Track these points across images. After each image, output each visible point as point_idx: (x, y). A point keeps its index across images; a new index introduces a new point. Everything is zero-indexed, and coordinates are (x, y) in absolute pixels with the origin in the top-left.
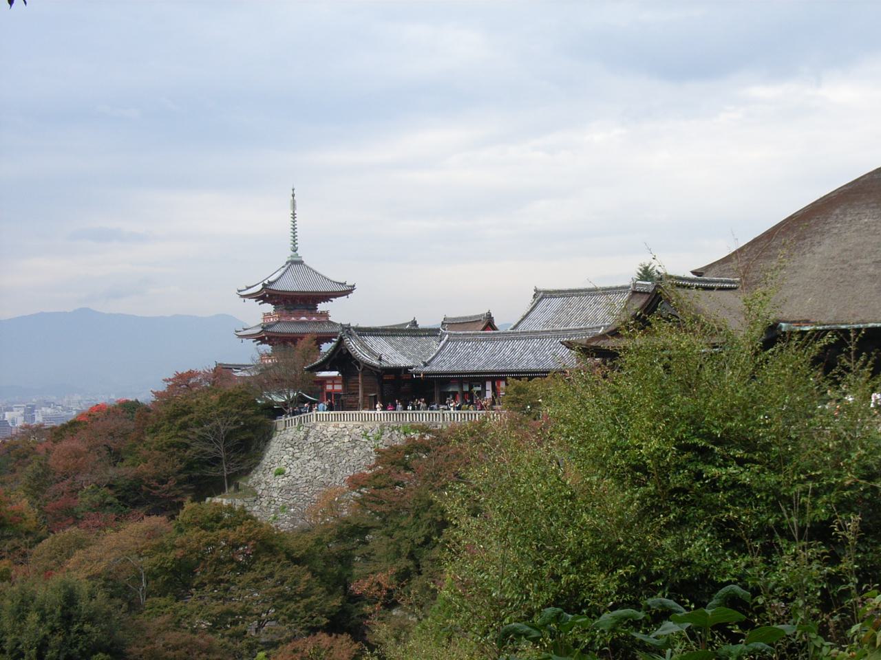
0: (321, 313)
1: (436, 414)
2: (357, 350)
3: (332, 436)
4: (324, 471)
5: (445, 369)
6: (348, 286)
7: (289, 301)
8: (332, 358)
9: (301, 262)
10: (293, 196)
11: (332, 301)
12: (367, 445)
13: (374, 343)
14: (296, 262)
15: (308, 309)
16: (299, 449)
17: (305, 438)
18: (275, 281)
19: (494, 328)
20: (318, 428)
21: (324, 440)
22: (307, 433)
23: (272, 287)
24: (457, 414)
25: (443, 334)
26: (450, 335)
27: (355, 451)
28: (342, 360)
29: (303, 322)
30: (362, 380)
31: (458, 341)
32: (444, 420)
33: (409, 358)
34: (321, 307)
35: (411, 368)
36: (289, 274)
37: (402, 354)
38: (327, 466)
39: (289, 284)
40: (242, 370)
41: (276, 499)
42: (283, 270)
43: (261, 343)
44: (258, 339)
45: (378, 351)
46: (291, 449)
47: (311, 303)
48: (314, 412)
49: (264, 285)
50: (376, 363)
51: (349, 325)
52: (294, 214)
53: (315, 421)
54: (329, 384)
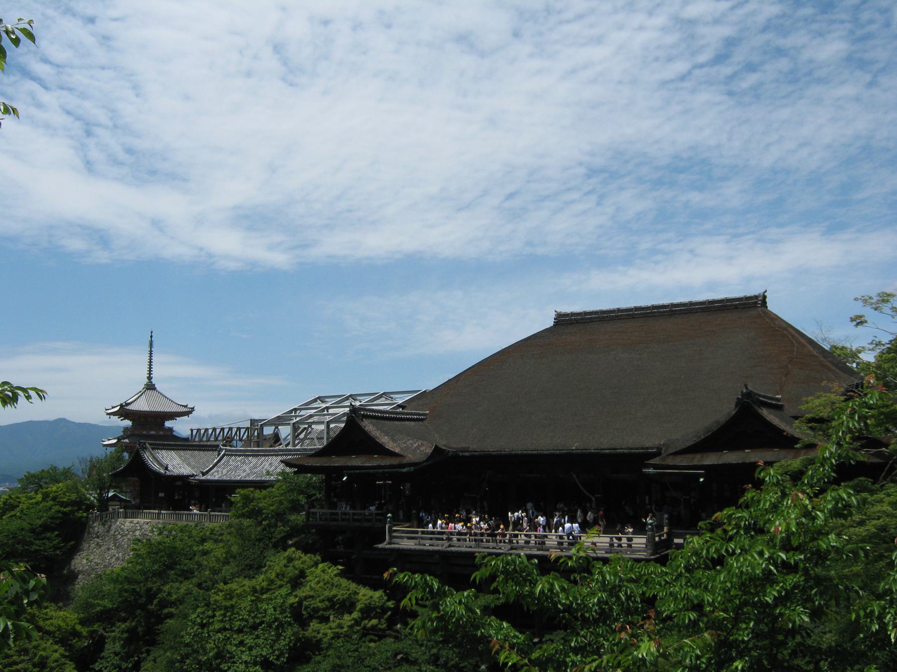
4: (118, 559)
5: (216, 478)
14: (150, 387)
20: (118, 523)
23: (129, 407)
25: (221, 450)
26: (226, 450)
31: (232, 455)
33: (193, 468)
34: (168, 424)
39: (142, 406)
45: (165, 462)
50: (162, 471)
52: (151, 351)
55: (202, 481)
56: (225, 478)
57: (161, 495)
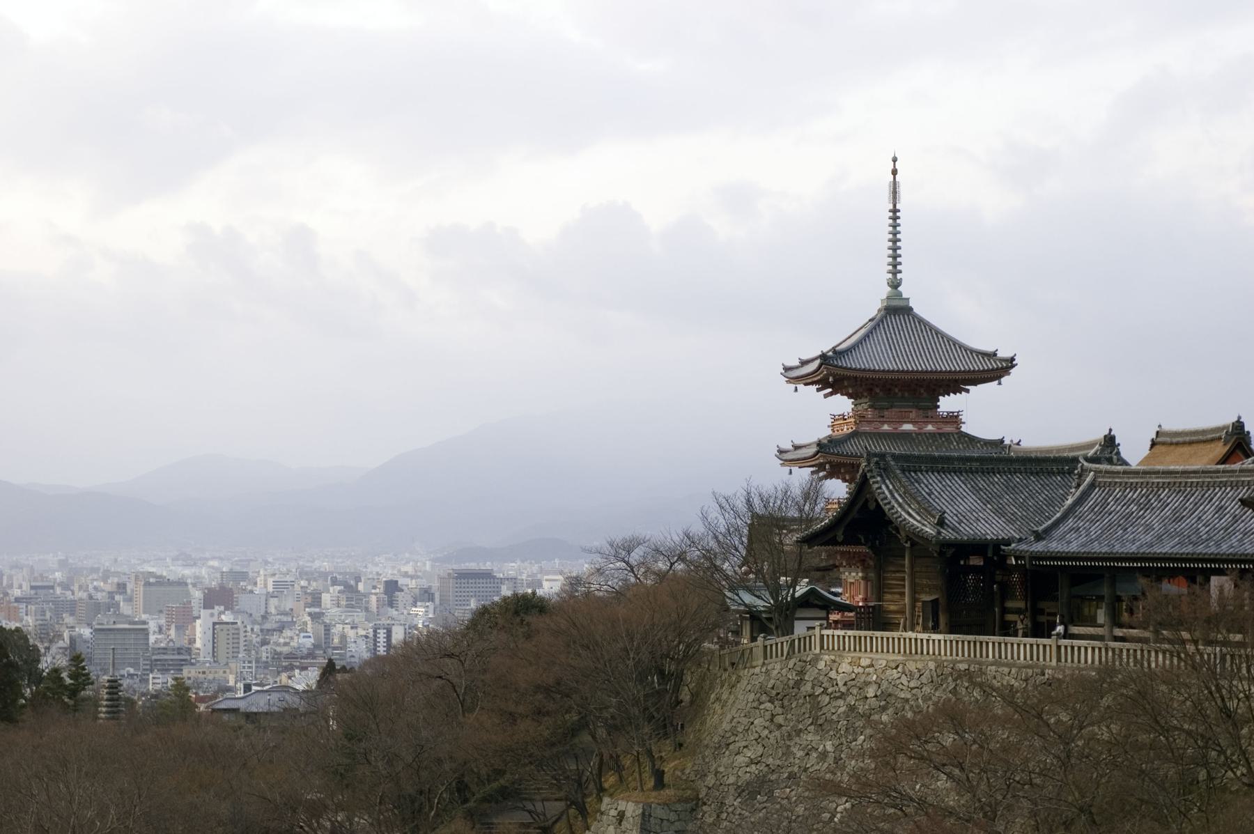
1: (1079, 648)
2: (893, 502)
4: (824, 755)
5: (1074, 547)
6: (1002, 360)
7: (878, 390)
8: (849, 518)
10: (894, 172)
11: (968, 391)
12: (907, 707)
13: (937, 487)
16: (783, 707)
17: (798, 684)
20: (821, 665)
21: (830, 690)
22: (801, 673)
24: (1086, 649)
25: (1084, 471)
26: (1097, 472)
29: (907, 435)
30: (912, 566)
32: (1059, 660)
33: (1010, 522)
34: (947, 404)
35: (1008, 542)
36: (880, 335)
37: (996, 512)
38: (829, 748)
45: (941, 503)
46: (768, 705)
48: (817, 631)
51: (1002, 441)
52: (895, 211)
53: (818, 651)
56: (1098, 548)
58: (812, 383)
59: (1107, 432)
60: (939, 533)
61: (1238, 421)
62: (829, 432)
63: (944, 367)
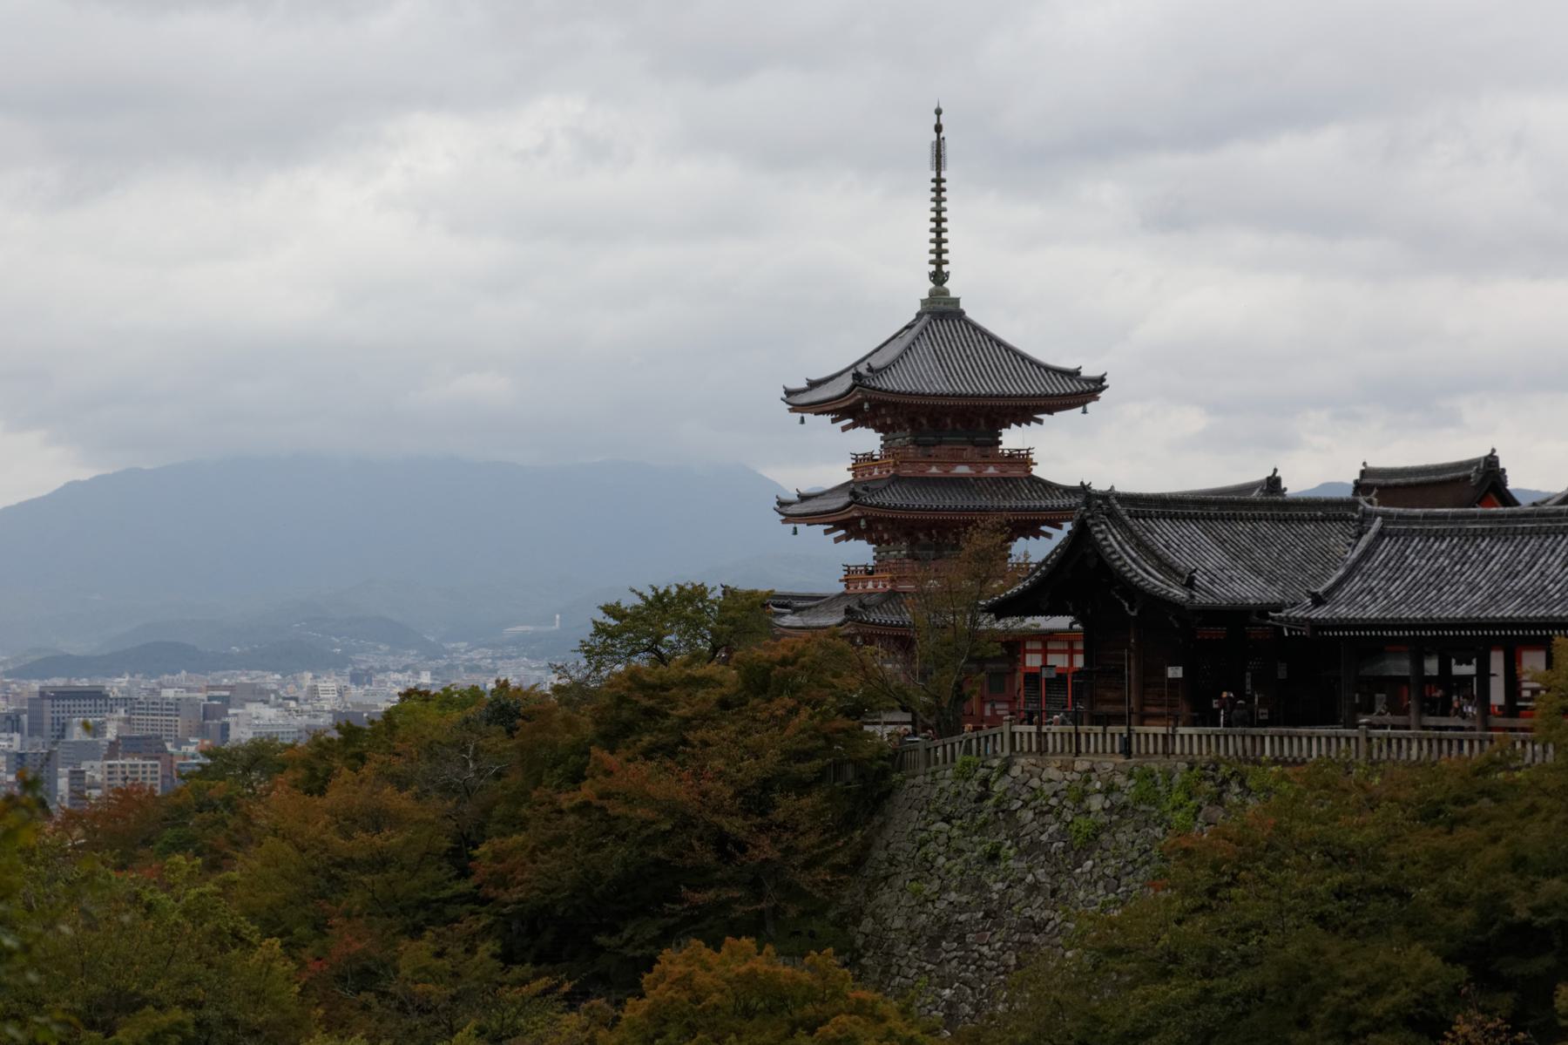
0: (1011, 455)
3: (1055, 795)
4: (1035, 888)
5: (1373, 612)
6: (1088, 380)
7: (924, 421)
9: (960, 315)
10: (938, 129)
11: (1040, 422)
14: (942, 312)
15: (976, 445)
18: (887, 368)
19: (1507, 499)
20: (1016, 771)
22: (985, 782)
25: (1368, 517)
26: (1385, 516)
27: (1121, 837)
28: (1081, 579)
29: (961, 481)
31: (1410, 534)
32: (1370, 753)
33: (1269, 582)
34: (1012, 438)
35: (1278, 608)
36: (924, 348)
39: (924, 377)
40: (796, 610)
41: (903, 963)
42: (909, 337)
43: (847, 538)
44: (838, 525)
45: (1183, 561)
47: (983, 427)
48: (1006, 727)
49: (857, 376)
50: (1178, 593)
52: (939, 181)
53: (1007, 752)
54: (1032, 651)
55: (1318, 626)
56: (1405, 613)
57: (1175, 672)
58: (823, 413)
59: (1270, 474)
60: (1192, 597)
61: (1491, 455)
62: (849, 477)
63: (1014, 389)
